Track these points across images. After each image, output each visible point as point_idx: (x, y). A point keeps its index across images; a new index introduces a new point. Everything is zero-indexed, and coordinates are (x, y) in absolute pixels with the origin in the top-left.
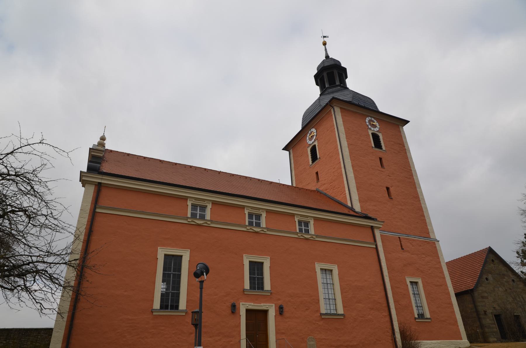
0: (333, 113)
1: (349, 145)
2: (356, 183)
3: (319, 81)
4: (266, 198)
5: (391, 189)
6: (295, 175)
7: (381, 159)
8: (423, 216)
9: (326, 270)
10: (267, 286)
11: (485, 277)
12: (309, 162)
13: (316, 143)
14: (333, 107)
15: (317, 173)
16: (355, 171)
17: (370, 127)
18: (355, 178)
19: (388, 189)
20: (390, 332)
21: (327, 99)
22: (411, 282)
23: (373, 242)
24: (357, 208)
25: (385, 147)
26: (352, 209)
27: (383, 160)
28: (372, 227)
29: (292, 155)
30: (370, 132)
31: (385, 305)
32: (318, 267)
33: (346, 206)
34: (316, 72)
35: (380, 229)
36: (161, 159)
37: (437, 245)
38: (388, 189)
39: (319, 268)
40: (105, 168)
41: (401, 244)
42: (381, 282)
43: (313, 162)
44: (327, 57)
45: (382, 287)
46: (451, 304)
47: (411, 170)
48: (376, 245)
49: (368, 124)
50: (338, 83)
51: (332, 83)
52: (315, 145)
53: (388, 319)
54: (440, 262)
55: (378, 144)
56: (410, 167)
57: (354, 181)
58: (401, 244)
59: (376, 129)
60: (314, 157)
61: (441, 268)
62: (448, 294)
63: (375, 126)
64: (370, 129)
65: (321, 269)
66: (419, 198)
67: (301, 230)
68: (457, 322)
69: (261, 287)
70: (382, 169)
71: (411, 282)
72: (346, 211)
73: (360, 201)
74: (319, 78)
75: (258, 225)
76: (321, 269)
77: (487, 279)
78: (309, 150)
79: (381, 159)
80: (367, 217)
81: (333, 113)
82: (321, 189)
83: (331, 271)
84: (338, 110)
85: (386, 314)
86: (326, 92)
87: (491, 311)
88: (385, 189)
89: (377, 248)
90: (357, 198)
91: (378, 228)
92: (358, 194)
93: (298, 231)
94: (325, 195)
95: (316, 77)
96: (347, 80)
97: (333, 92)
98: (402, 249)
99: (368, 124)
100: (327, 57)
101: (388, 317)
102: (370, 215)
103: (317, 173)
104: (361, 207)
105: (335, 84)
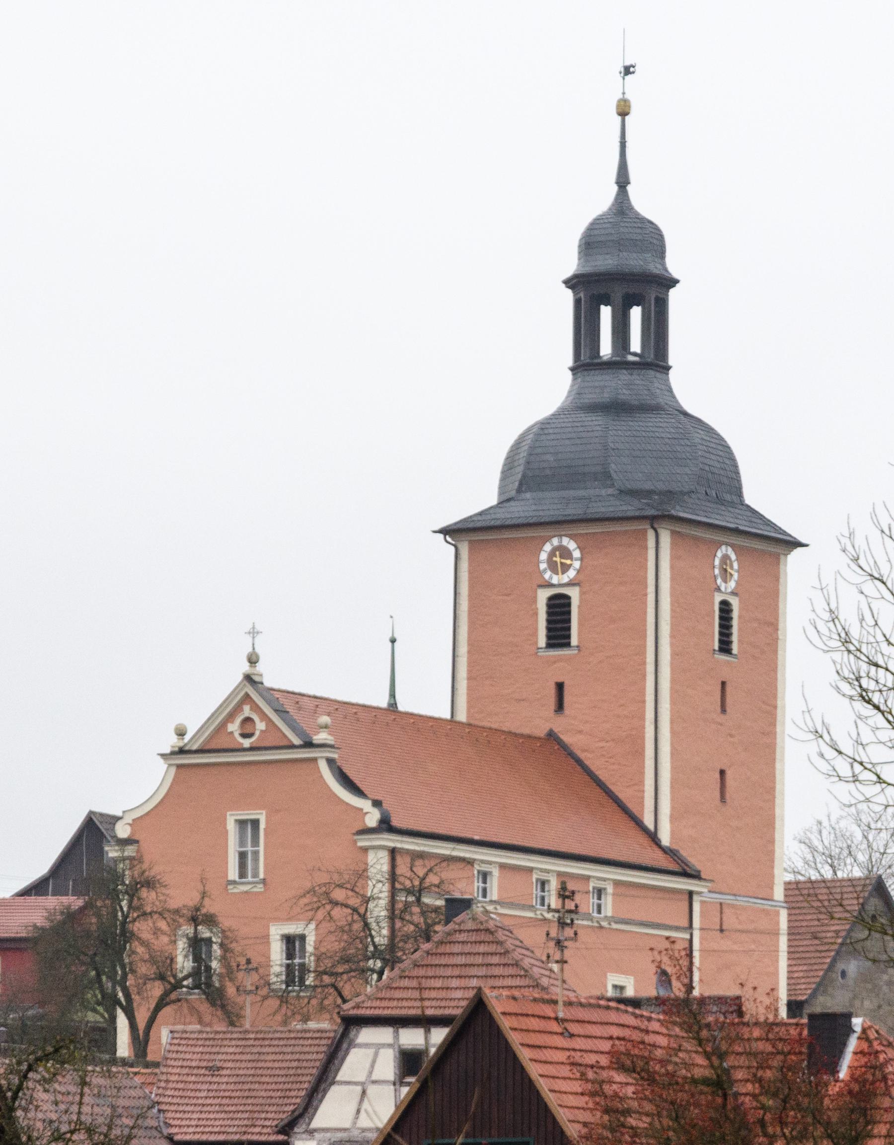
0: (651, 543)
1: (674, 654)
5: (729, 775)
6: (470, 644)
7: (723, 684)
8: (772, 841)
11: (840, 966)
12: (535, 634)
13: (574, 594)
15: (560, 687)
24: (665, 838)
25: (739, 647)
27: (729, 689)
29: (464, 566)
30: (718, 598)
41: (721, 919)
43: (549, 646)
44: (623, 203)
47: (775, 707)
49: (717, 571)
56: (775, 696)
58: (721, 919)
60: (559, 634)
64: (718, 589)
70: (721, 718)
77: (844, 974)
78: (543, 596)
79: (723, 684)
81: (651, 543)
82: (566, 738)
84: (666, 539)
94: (579, 762)
100: (623, 203)
103: (560, 687)
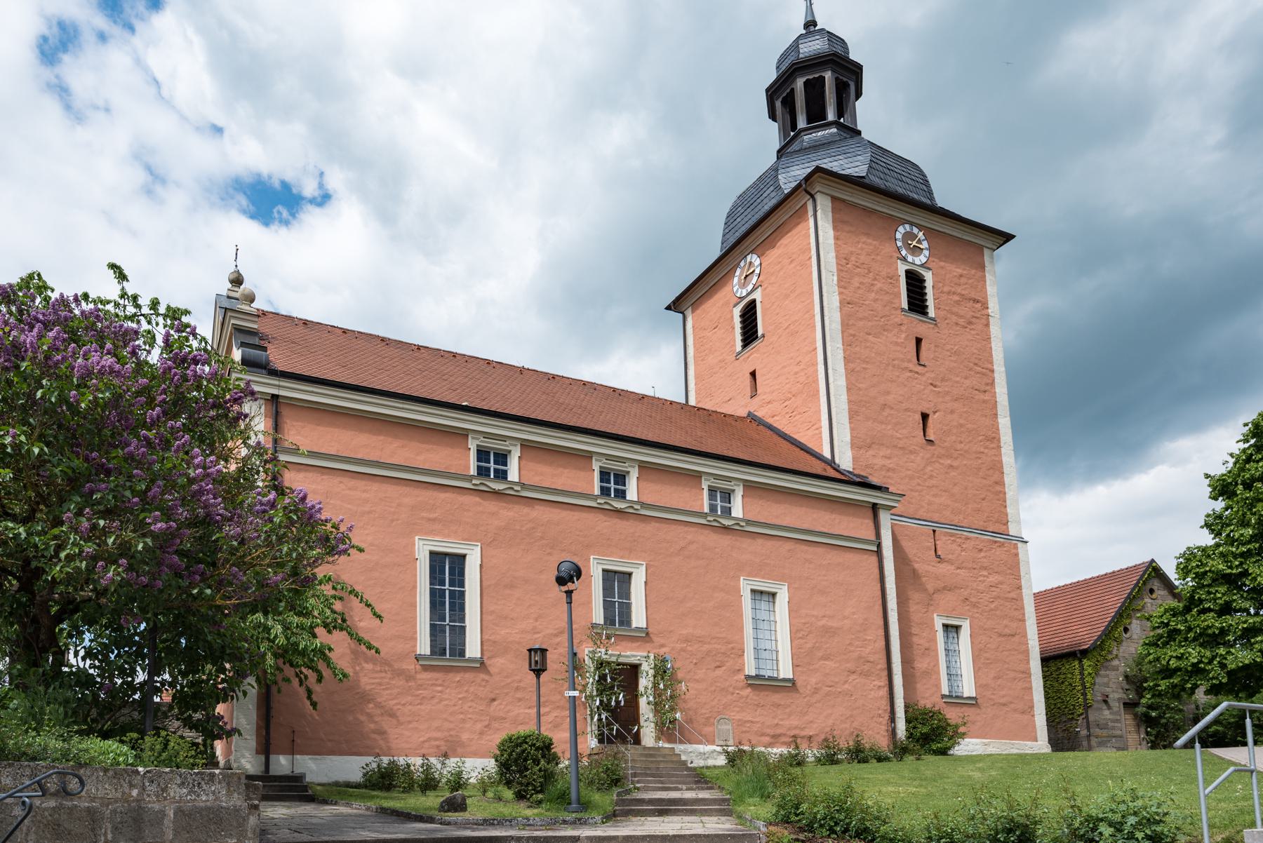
1: (844, 303)
2: (850, 402)
3: (778, 104)
4: (638, 436)
7: (919, 341)
9: (762, 592)
10: (639, 619)
14: (812, 196)
16: (850, 372)
17: (904, 252)
18: (849, 390)
19: (925, 417)
20: (887, 716)
21: (797, 172)
22: (946, 626)
23: (873, 538)
24: (845, 461)
26: (831, 463)
28: (875, 508)
31: (884, 665)
32: (745, 586)
33: (819, 457)
34: (772, 76)
35: (893, 511)
36: (382, 334)
37: (1020, 550)
38: (925, 417)
39: (749, 588)
40: (278, 357)
42: (881, 622)
45: (881, 632)
46: (1027, 673)
48: (879, 546)
50: (831, 116)
51: (816, 115)
52: (754, 301)
53: (884, 692)
54: (1020, 588)
55: (917, 303)
57: (844, 397)
59: (922, 259)
61: (1019, 599)
62: (1026, 652)
63: (916, 250)
65: (753, 591)
66: (999, 441)
67: (713, 508)
68: (1032, 707)
69: (626, 620)
71: (946, 626)
72: (818, 468)
73: (853, 445)
74: (779, 97)
75: (621, 494)
76: (753, 591)
79: (919, 341)
80: (865, 485)
83: (774, 595)
85: (884, 682)
86: (795, 146)
87: (1116, 696)
88: (918, 417)
89: (879, 553)
90: (848, 438)
91: (890, 508)
92: (852, 429)
93: (706, 510)
95: (772, 93)
96: (859, 104)
97: (816, 147)
98: (938, 557)
99: (899, 244)
101: (886, 689)
102: (874, 480)
104: (855, 459)
105: (824, 117)
